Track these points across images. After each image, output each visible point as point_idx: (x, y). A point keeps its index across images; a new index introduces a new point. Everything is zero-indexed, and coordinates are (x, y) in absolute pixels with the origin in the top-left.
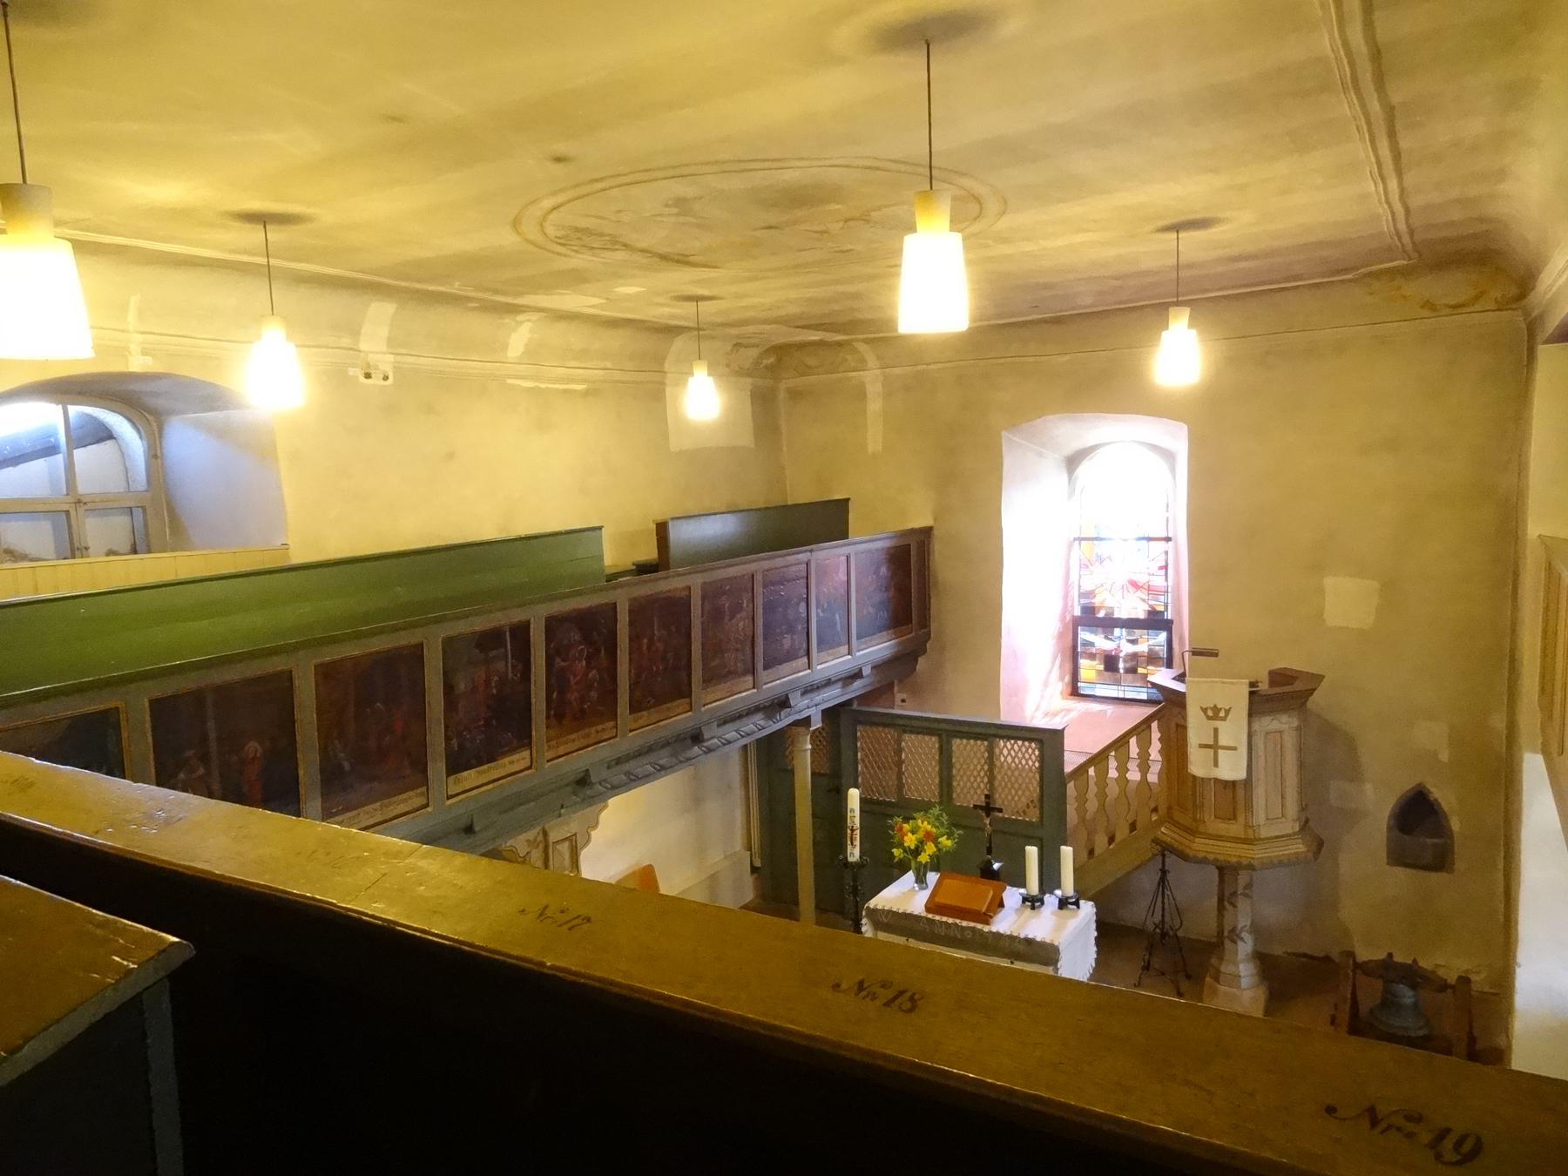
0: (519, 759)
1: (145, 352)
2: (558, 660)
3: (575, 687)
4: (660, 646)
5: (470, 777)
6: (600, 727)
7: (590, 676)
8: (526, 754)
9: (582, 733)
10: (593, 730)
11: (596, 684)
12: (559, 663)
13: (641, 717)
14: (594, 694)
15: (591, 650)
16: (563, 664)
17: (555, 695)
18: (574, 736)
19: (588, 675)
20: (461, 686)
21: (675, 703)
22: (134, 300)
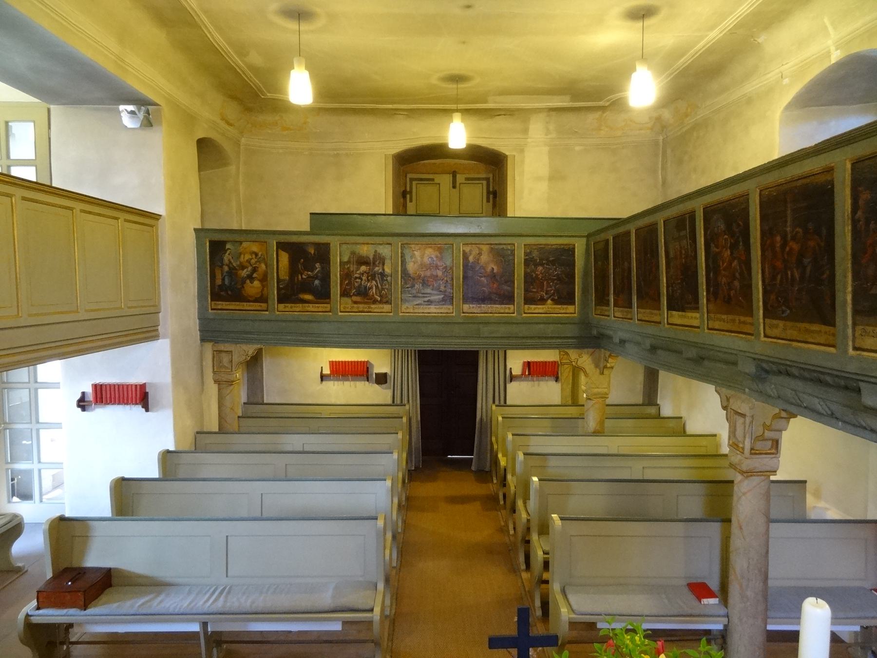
0: (692, 318)
1: (837, 49)
2: (712, 245)
3: (723, 272)
4: (795, 246)
5: (677, 317)
6: (743, 319)
7: (733, 265)
8: (697, 315)
9: (730, 317)
10: (737, 318)
11: (737, 275)
12: (714, 249)
13: (777, 326)
14: (736, 283)
15: (732, 241)
16: (717, 250)
17: (711, 275)
18: (724, 317)
19: (731, 264)
20: (672, 255)
21: (815, 327)
22: (826, 21)
